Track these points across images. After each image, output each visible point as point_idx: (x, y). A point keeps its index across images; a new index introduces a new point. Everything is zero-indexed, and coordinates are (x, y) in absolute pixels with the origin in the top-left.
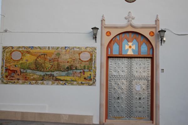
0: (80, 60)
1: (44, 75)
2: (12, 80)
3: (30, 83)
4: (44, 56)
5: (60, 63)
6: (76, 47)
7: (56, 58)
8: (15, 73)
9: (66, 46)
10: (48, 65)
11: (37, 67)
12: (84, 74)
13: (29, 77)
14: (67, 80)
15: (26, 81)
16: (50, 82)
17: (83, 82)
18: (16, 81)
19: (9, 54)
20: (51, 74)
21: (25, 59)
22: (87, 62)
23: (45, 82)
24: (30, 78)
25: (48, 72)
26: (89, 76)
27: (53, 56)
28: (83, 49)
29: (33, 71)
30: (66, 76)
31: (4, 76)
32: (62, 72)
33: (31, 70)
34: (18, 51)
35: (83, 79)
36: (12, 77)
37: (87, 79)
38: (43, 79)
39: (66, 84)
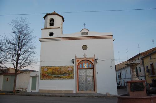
3: (51, 79)
10: (57, 72)
16: (58, 79)
21: (49, 71)
23: (56, 79)
27: (58, 70)
38: (55, 77)
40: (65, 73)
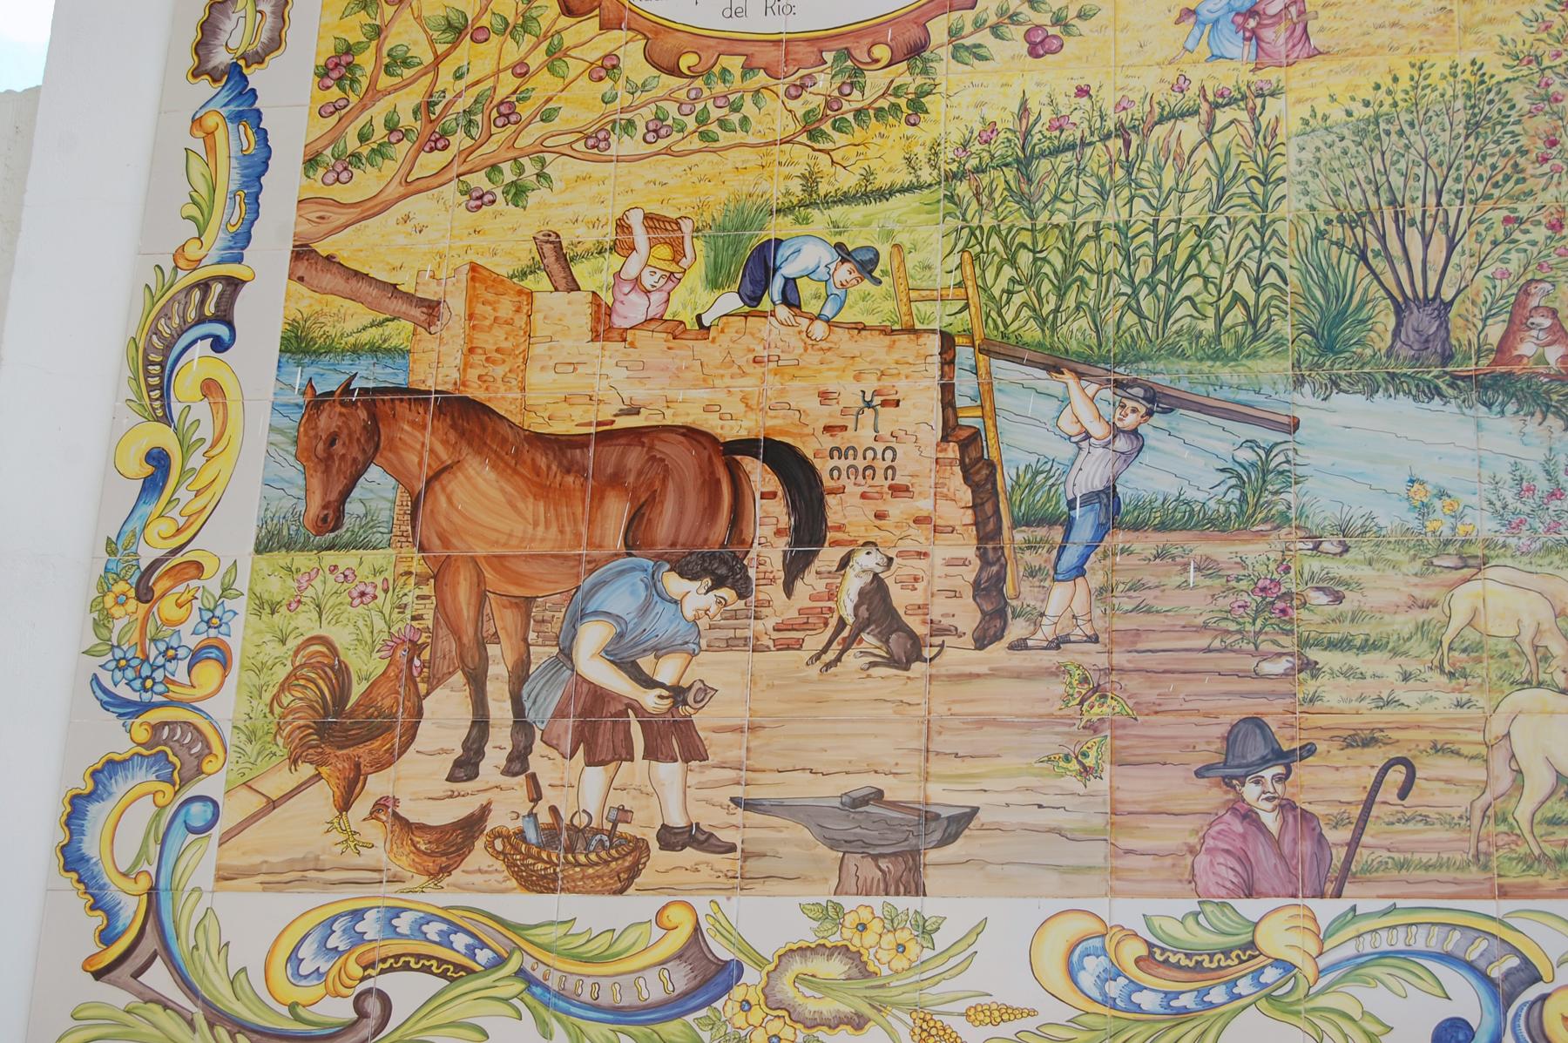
2: (611, 857)
8: (724, 569)
13: (1430, 701)
15: (1279, 927)
18: (765, 921)
24: (1446, 787)
31: (225, 703)
33: (1497, 384)
36: (598, 729)
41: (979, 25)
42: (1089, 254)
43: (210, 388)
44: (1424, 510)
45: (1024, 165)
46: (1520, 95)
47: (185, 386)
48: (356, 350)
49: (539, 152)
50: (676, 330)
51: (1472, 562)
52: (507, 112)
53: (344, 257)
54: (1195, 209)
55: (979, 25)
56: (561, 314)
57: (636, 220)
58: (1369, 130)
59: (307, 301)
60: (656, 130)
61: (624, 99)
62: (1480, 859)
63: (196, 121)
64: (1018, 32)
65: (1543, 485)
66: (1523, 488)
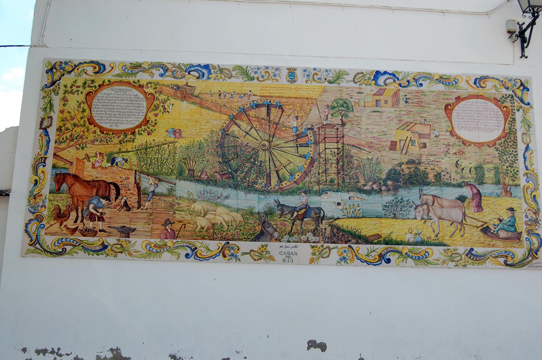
0: (453, 140)
1: (269, 213)
2: (93, 233)
3: (194, 254)
4: (268, 114)
5: (354, 151)
6: (428, 76)
7: (332, 126)
8: (108, 198)
9: (382, 70)
10: (290, 159)
11: (234, 166)
12: (479, 207)
14: (394, 237)
15: (169, 242)
16: (304, 250)
17: (479, 250)
18: (111, 241)
19: (81, 98)
20: (307, 207)
21: (164, 123)
22: (492, 150)
23: (273, 247)
24: (189, 227)
25: (292, 192)
26: (506, 217)
27: (314, 117)
28: (462, 84)
29: (209, 188)
30: (386, 217)
31: (45, 213)
32: (364, 196)
33: (199, 180)
34: (129, 83)
35: (477, 233)
36: (92, 217)
37: (496, 236)
39: (388, 261)
40: (397, 180)
41: (142, 130)
42: (153, 161)
43: (43, 172)
44: (189, 195)
45: (146, 149)
46: (205, 144)
47: (39, 171)
48: (62, 168)
49: (86, 143)
50: (102, 168)
51: (194, 202)
52: (82, 137)
53: (60, 155)
54: (166, 156)
55: (142, 130)
56: (88, 165)
57: (98, 153)
58: (187, 148)
59: (55, 161)
60: (101, 141)
61: (97, 136)
62: (192, 236)
63: (40, 135)
64: (146, 132)
65: (203, 193)
66: (201, 193)
